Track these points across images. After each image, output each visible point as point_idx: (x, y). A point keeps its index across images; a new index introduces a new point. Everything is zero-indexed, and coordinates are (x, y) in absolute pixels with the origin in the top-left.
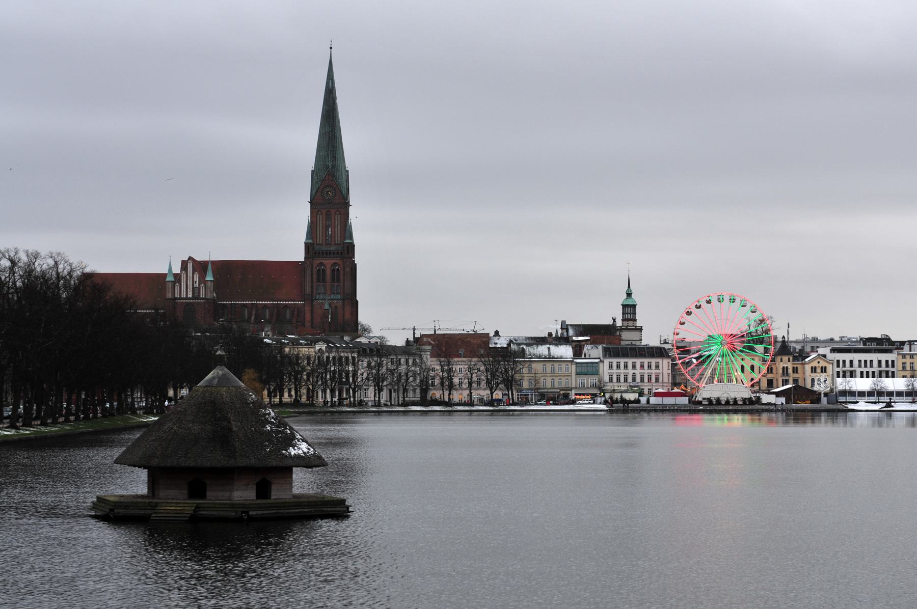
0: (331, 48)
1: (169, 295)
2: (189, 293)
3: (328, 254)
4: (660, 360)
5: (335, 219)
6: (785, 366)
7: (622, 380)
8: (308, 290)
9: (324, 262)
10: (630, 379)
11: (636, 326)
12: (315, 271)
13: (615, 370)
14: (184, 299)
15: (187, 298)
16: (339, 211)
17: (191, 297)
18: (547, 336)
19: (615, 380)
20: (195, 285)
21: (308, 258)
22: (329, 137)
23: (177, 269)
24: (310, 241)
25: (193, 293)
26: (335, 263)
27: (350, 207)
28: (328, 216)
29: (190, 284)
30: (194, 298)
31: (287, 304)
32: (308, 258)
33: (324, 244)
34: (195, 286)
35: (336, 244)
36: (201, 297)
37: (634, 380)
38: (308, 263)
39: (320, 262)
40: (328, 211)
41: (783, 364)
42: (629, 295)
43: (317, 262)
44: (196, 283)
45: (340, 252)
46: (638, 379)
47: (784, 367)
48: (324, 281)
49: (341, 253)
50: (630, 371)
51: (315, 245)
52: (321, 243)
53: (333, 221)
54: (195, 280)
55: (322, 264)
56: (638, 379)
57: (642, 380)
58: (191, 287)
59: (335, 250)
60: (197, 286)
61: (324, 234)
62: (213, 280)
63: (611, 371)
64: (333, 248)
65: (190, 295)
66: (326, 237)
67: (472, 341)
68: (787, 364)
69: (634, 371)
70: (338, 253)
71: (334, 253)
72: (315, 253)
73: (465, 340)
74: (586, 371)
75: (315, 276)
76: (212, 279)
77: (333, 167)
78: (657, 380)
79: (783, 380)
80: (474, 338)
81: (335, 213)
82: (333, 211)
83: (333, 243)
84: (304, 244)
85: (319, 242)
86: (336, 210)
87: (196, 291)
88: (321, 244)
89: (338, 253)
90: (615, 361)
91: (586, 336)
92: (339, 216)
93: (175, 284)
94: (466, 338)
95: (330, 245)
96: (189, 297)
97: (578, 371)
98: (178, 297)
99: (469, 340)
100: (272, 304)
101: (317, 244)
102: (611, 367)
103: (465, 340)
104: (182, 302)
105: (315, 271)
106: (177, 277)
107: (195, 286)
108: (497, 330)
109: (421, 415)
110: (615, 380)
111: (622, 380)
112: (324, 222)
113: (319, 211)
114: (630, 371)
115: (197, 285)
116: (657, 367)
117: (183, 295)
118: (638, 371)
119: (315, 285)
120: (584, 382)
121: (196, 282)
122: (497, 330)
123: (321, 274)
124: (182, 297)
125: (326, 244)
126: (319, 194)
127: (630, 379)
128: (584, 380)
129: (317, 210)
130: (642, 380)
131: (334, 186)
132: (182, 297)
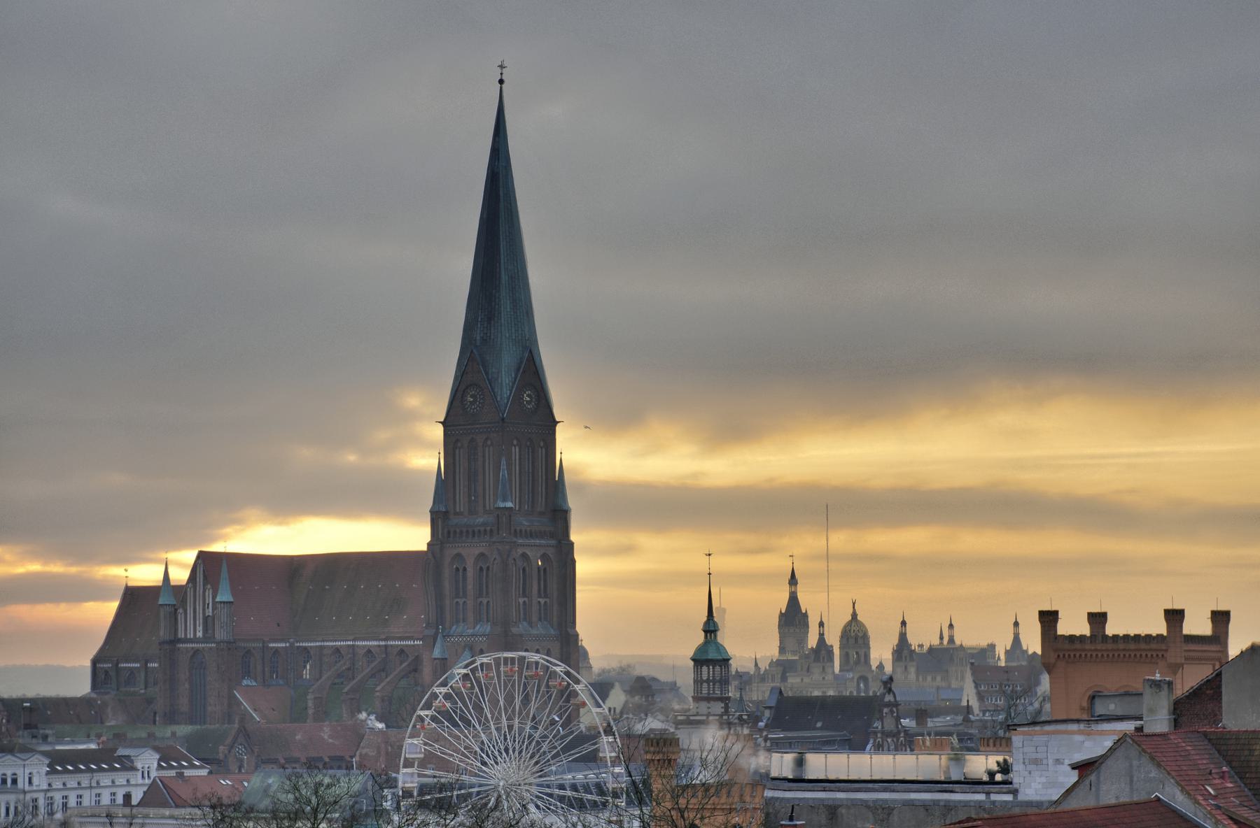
0: (501, 82)
5: (484, 456)
14: (191, 641)
17: (201, 636)
20: (207, 611)
25: (205, 630)
26: (482, 555)
27: (559, 428)
30: (205, 639)
43: (450, 552)
44: (208, 608)
54: (207, 602)
58: (201, 615)
60: (211, 614)
65: (200, 634)
72: (449, 533)
85: (460, 509)
93: (176, 610)
96: (198, 636)
98: (183, 636)
100: (379, 646)
101: (456, 514)
104: (187, 648)
113: (457, 440)
115: (209, 612)
117: (190, 635)
121: (208, 604)
124: (188, 637)
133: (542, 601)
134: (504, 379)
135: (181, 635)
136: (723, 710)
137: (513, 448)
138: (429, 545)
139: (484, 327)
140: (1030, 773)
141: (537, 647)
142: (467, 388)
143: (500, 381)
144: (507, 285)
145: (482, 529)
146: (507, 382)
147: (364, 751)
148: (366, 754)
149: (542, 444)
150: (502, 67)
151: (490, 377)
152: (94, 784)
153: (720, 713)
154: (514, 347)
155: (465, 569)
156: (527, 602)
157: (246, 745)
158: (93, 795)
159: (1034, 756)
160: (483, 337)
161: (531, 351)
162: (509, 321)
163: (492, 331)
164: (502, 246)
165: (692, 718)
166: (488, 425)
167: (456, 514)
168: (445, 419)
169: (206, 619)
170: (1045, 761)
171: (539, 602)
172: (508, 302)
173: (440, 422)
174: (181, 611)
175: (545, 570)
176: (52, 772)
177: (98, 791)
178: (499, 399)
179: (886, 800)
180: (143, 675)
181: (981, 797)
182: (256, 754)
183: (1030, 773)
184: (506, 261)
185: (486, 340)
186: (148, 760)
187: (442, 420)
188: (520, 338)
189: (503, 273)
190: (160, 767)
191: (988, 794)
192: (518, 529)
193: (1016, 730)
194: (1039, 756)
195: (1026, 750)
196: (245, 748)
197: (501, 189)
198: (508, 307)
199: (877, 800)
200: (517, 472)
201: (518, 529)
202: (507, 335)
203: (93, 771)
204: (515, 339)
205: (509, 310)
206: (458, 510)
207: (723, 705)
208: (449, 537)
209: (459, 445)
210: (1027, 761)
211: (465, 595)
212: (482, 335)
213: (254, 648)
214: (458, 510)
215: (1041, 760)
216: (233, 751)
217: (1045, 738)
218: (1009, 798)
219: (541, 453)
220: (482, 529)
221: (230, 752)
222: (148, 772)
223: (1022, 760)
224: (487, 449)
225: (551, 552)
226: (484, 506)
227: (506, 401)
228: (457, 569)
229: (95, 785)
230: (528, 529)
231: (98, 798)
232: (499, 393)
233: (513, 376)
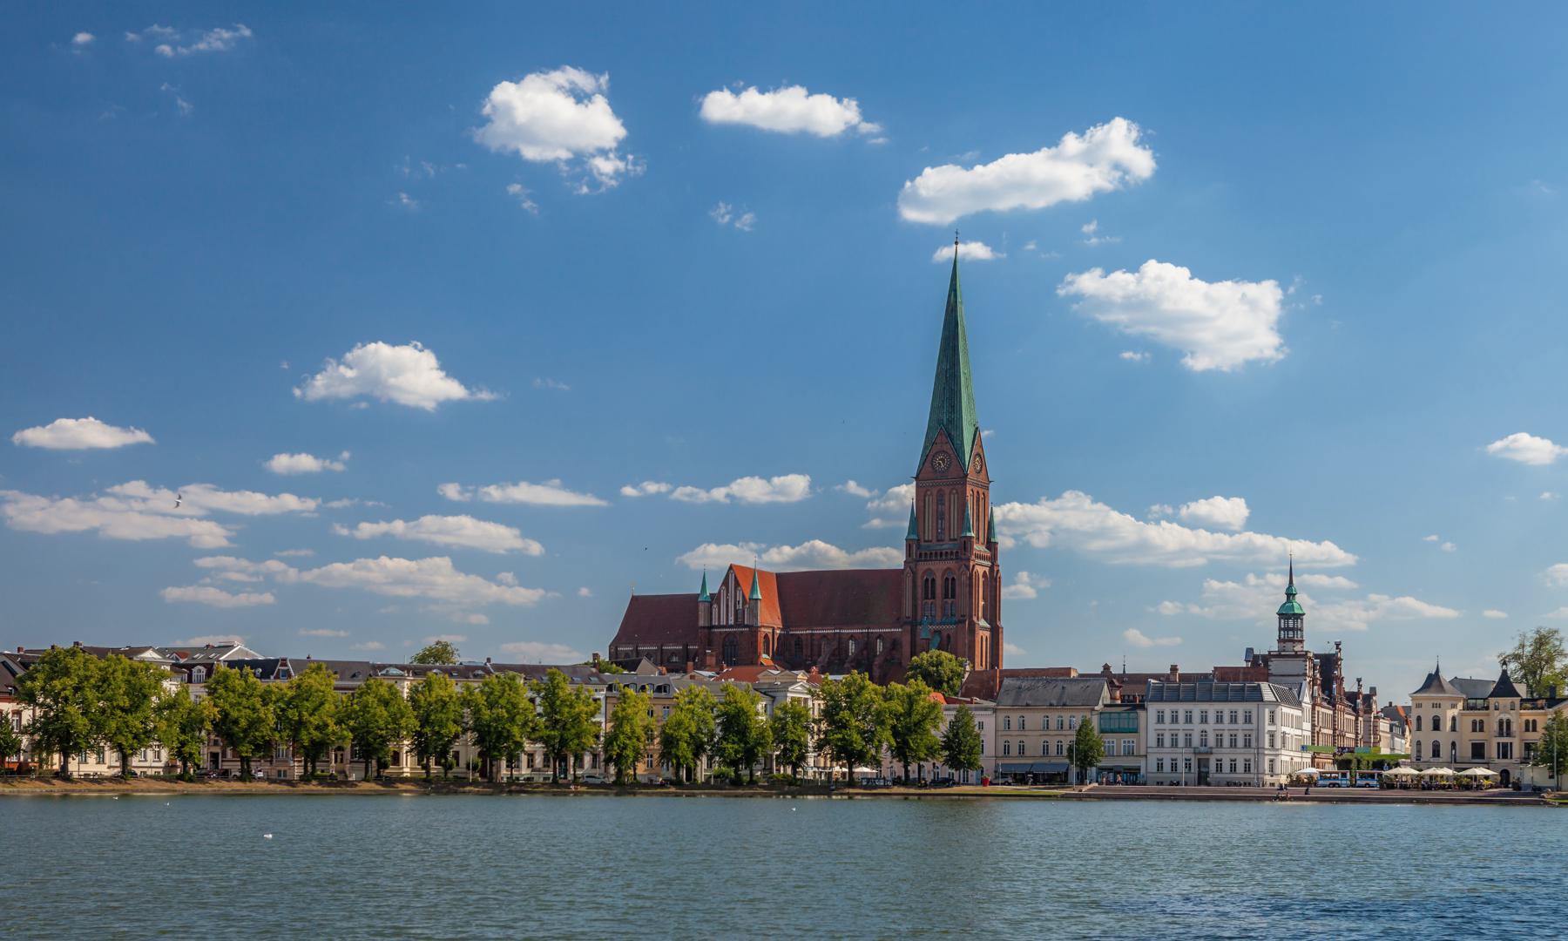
1: (702, 623)
2: (730, 618)
3: (941, 555)
4: (1251, 706)
6: (1505, 717)
7: (1181, 743)
8: (908, 612)
9: (933, 568)
10: (1196, 742)
12: (920, 583)
13: (1167, 725)
15: (731, 627)
16: (957, 490)
18: (1169, 672)
19: (1226, 743)
21: (909, 562)
22: (946, 377)
23: (713, 588)
24: (914, 537)
26: (948, 569)
28: (940, 500)
29: (731, 604)
30: (736, 625)
31: (855, 633)
32: (909, 562)
33: (934, 541)
35: (951, 540)
36: (746, 623)
37: (1204, 743)
38: (908, 569)
39: (926, 567)
40: (940, 490)
41: (1500, 713)
42: (1290, 595)
43: (922, 566)
45: (954, 551)
46: (1211, 741)
47: (1501, 723)
48: (934, 597)
49: (957, 552)
50: (1197, 727)
51: (922, 543)
52: (930, 538)
53: (947, 504)
56: (1211, 741)
57: (1219, 743)
59: (949, 549)
61: (935, 524)
63: (1160, 726)
64: (946, 546)
65: (731, 622)
66: (937, 530)
68: (1509, 714)
69: (1204, 727)
70: (952, 553)
71: (947, 553)
72: (921, 554)
74: (1117, 726)
75: (920, 590)
77: (950, 421)
78: (1247, 744)
79: (1499, 744)
81: (950, 493)
82: (947, 490)
83: (947, 538)
87: (740, 616)
88: (931, 541)
89: (952, 553)
90: (1168, 708)
92: (956, 496)
93: (711, 606)
95: (942, 540)
97: (1103, 727)
100: (862, 633)
101: (925, 541)
102: (1160, 719)
105: (920, 583)
106: (715, 598)
108: (1106, 664)
109: (306, 797)
110: (1167, 742)
111: (1181, 743)
112: (935, 508)
113: (928, 490)
114: (1197, 727)
115: (740, 606)
116: (1248, 720)
117: (723, 622)
118: (1211, 727)
119: (919, 602)
120: (1113, 747)
122: (1106, 664)
123: (930, 584)
125: (938, 541)
127: (1196, 742)
128: (1113, 742)
129: (925, 490)
130: (1219, 743)
131: (948, 451)
132: (722, 624)
135: (715, 623)
138: (905, 562)
142: (936, 453)
145: (949, 551)
148: (972, 687)
155: (933, 580)
167: (925, 541)
168: (918, 475)
169: (736, 611)
174: (715, 606)
180: (659, 654)
206: (926, 538)
209: (929, 493)
211: (933, 597)
214: (926, 538)
220: (949, 551)
224: (952, 496)
225: (987, 569)
226: (950, 535)
227: (967, 464)
228: (927, 580)
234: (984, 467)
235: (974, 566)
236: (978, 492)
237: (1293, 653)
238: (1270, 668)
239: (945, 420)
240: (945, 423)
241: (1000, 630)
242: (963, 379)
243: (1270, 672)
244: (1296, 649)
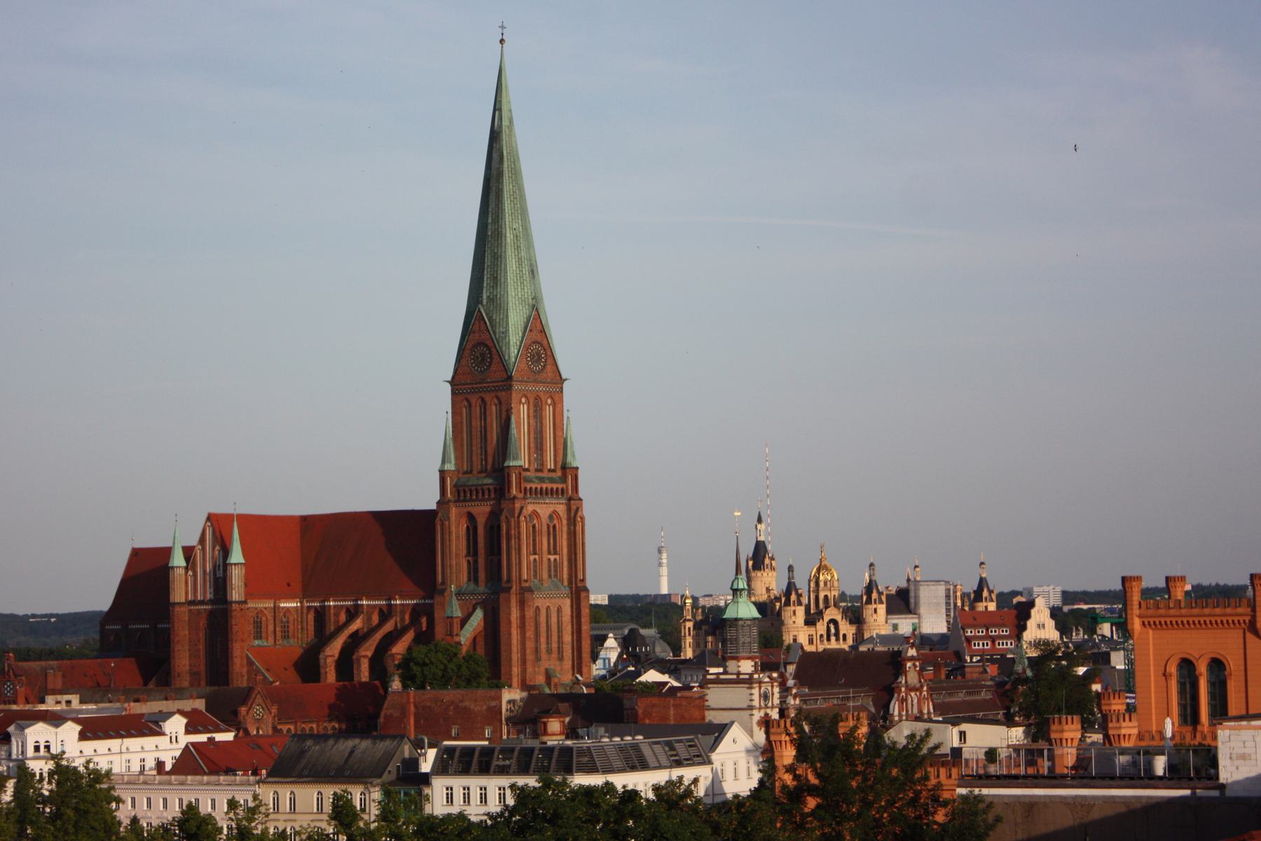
0: (502, 41)
11: (739, 674)
27: (566, 385)
34: (218, 576)
44: (219, 569)
55: (471, 517)
60: (221, 575)
62: (242, 561)
65: (209, 596)
67: (472, 707)
71: (489, 490)
73: (460, 704)
76: (242, 561)
80: (476, 701)
82: (488, 397)
84: (438, 473)
86: (493, 395)
91: (666, 691)
94: (461, 701)
99: (467, 703)
103: (460, 704)
104: (198, 610)
107: (218, 576)
126: (463, 362)
131: (488, 342)
132: (199, 598)
133: (552, 558)
134: (511, 338)
136: (753, 669)
137: (522, 405)
139: (490, 286)
140: (1237, 768)
141: (548, 604)
143: (507, 340)
144: (512, 244)
146: (515, 341)
147: (390, 711)
149: (549, 401)
150: (503, 27)
151: (497, 337)
152: (124, 750)
153: (750, 672)
154: (520, 306)
156: (538, 559)
157: (264, 706)
158: (124, 762)
159: (1242, 751)
160: (489, 296)
161: (537, 310)
162: (515, 281)
163: (499, 290)
164: (506, 205)
165: (722, 677)
166: (495, 384)
168: (453, 377)
170: (1253, 757)
171: (549, 559)
172: (514, 260)
173: (447, 381)
174: (190, 573)
175: (554, 527)
176: (83, 736)
177: (126, 757)
178: (507, 358)
179: (1084, 797)
181: (1187, 792)
182: (273, 715)
183: (1237, 768)
184: (511, 220)
185: (493, 299)
186: (176, 725)
187: (449, 379)
188: (526, 296)
189: (508, 231)
190: (188, 732)
191: (1193, 789)
192: (528, 487)
193: (1221, 724)
194: (1247, 751)
195: (1232, 744)
196: (263, 708)
197: (505, 148)
198: (514, 265)
199: (1076, 797)
200: (526, 430)
201: (528, 487)
202: (513, 294)
203: (122, 737)
204: (521, 298)
205: (514, 268)
207: (753, 664)
208: (459, 496)
210: (1234, 756)
212: (488, 294)
213: (265, 608)
215: (1250, 755)
216: (251, 712)
217: (1251, 732)
218: (1215, 793)
219: (548, 412)
221: (248, 713)
222: (176, 737)
223: (1228, 755)
225: (561, 509)
227: (513, 360)
229: (125, 751)
230: (539, 487)
231: (128, 764)
232: (507, 352)
233: (520, 334)
234: (550, 361)
235: (522, 508)
236: (537, 398)
237: (735, 677)
238: (707, 697)
239: (485, 297)
240: (485, 303)
241: (583, 594)
242: (509, 236)
243: (707, 704)
244: (743, 670)
